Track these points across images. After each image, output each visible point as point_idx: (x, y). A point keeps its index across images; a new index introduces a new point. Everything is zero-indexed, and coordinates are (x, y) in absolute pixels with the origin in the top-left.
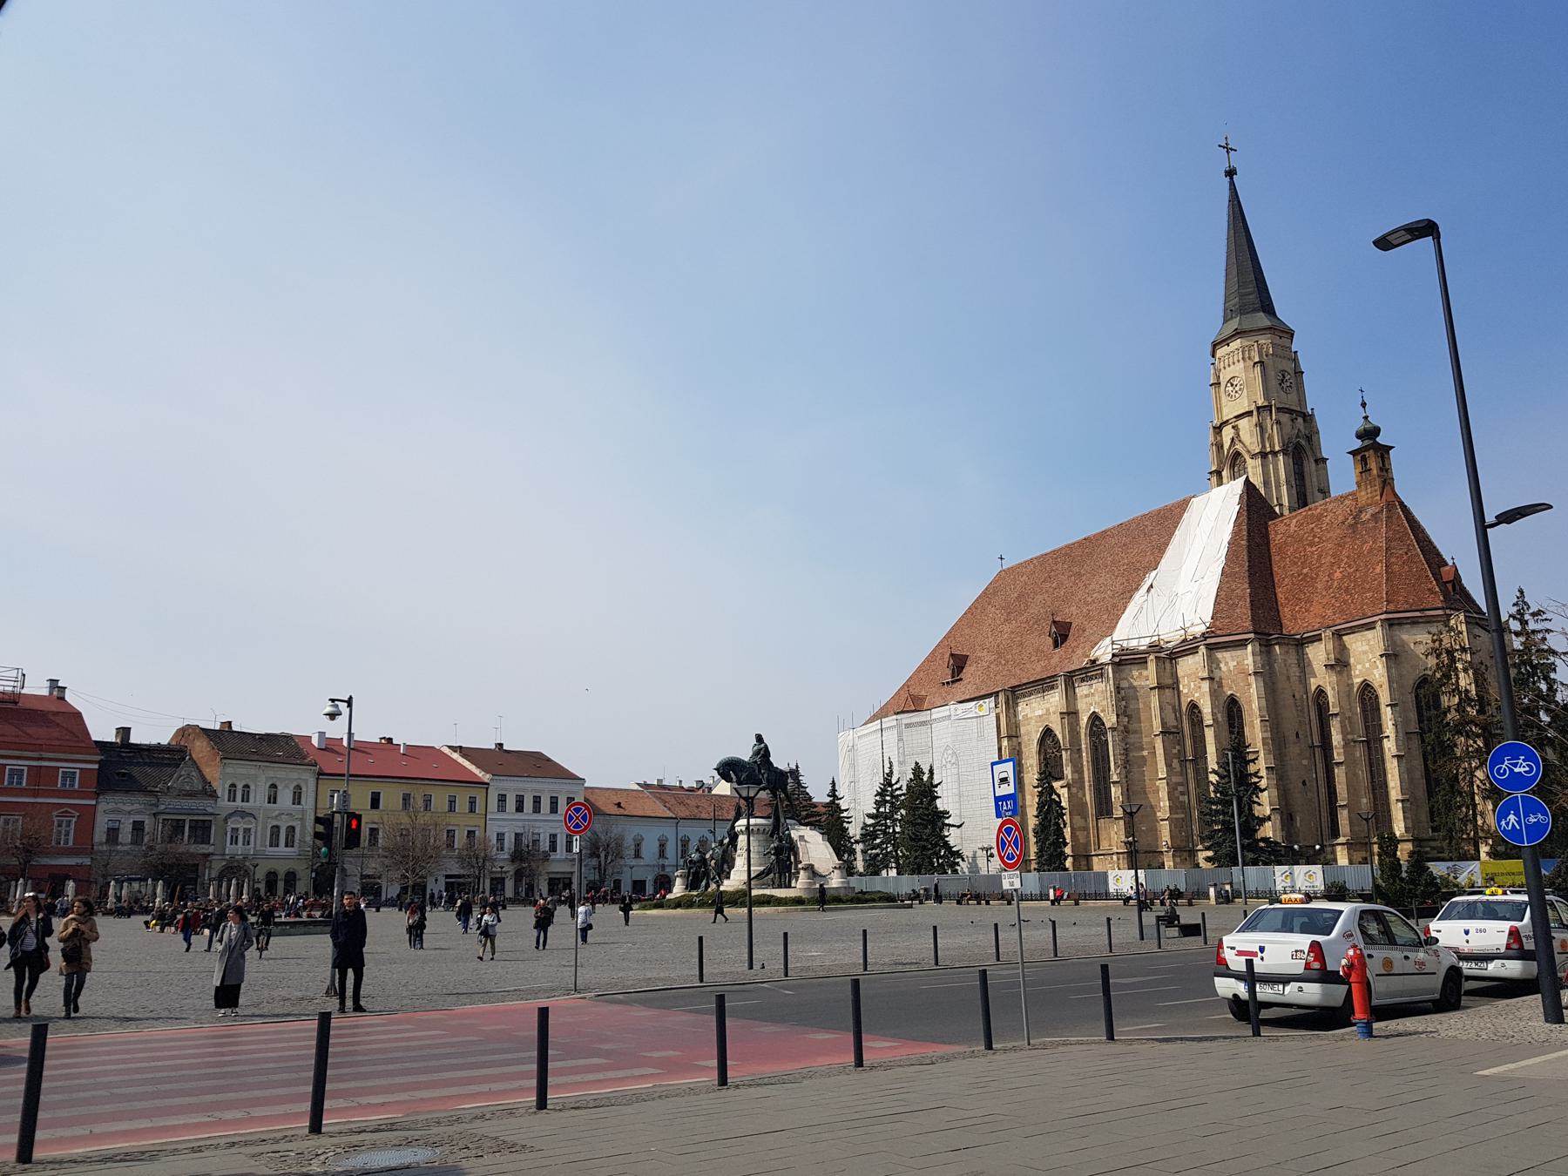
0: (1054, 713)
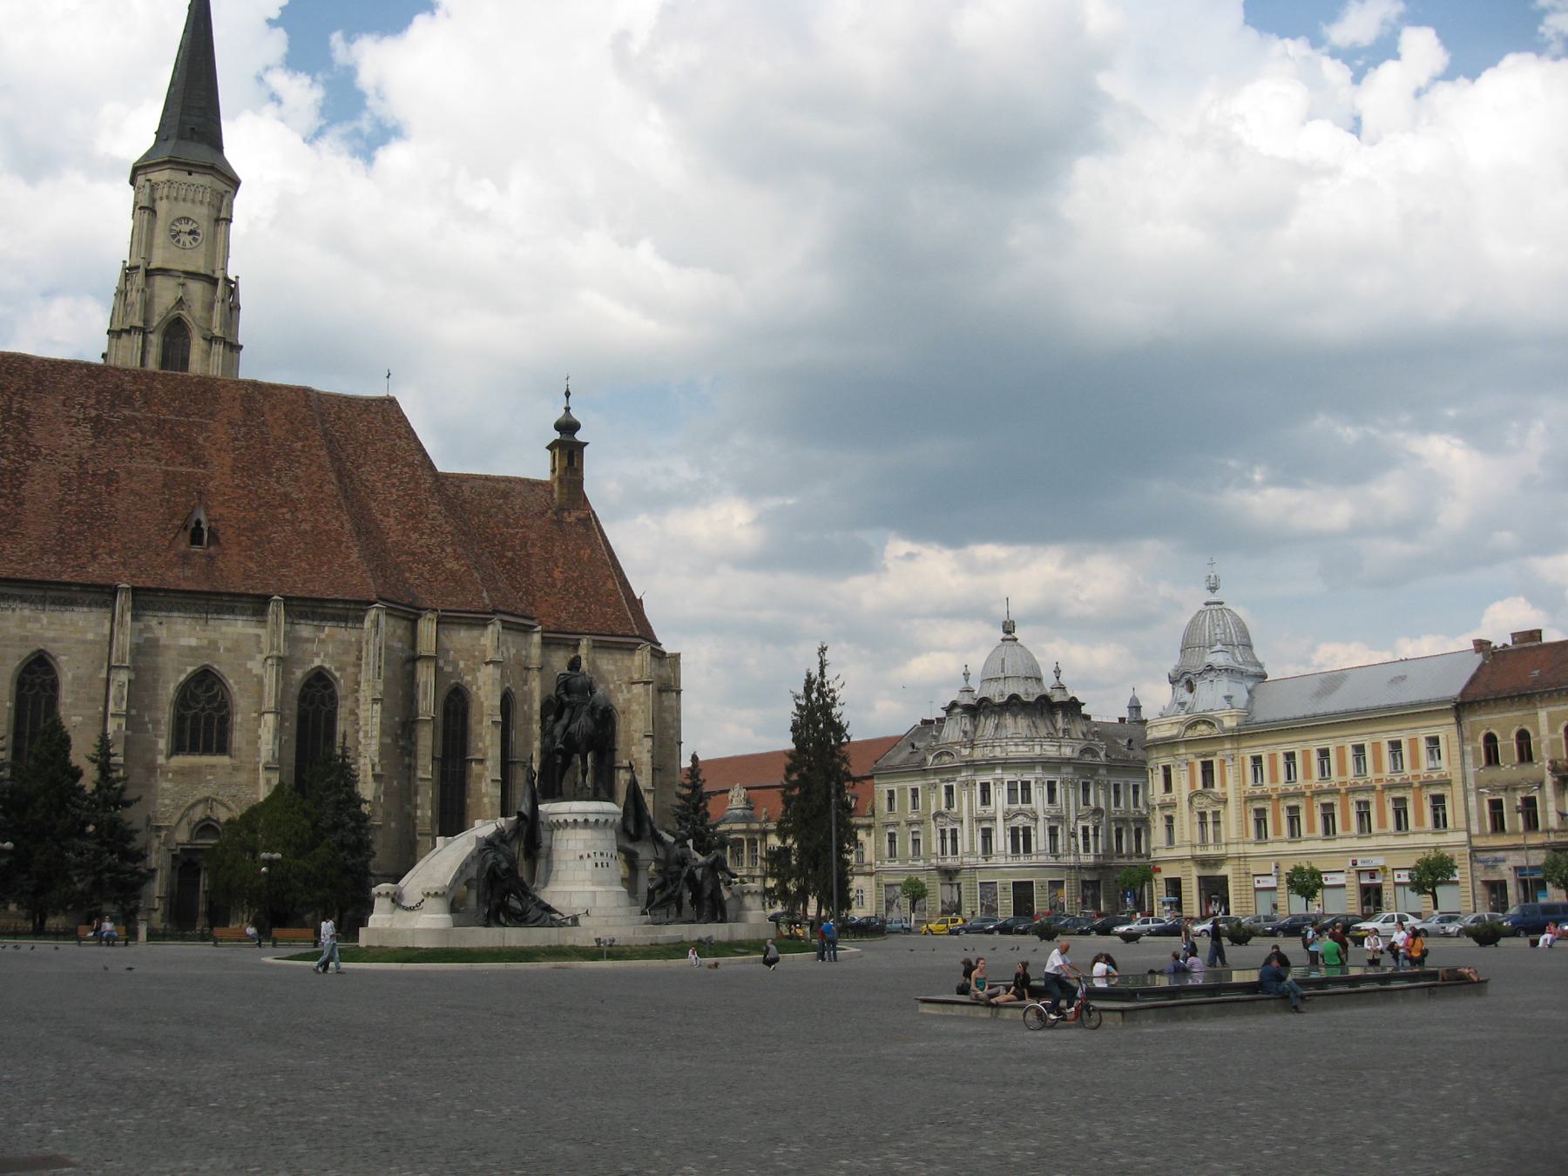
0: (228, 650)
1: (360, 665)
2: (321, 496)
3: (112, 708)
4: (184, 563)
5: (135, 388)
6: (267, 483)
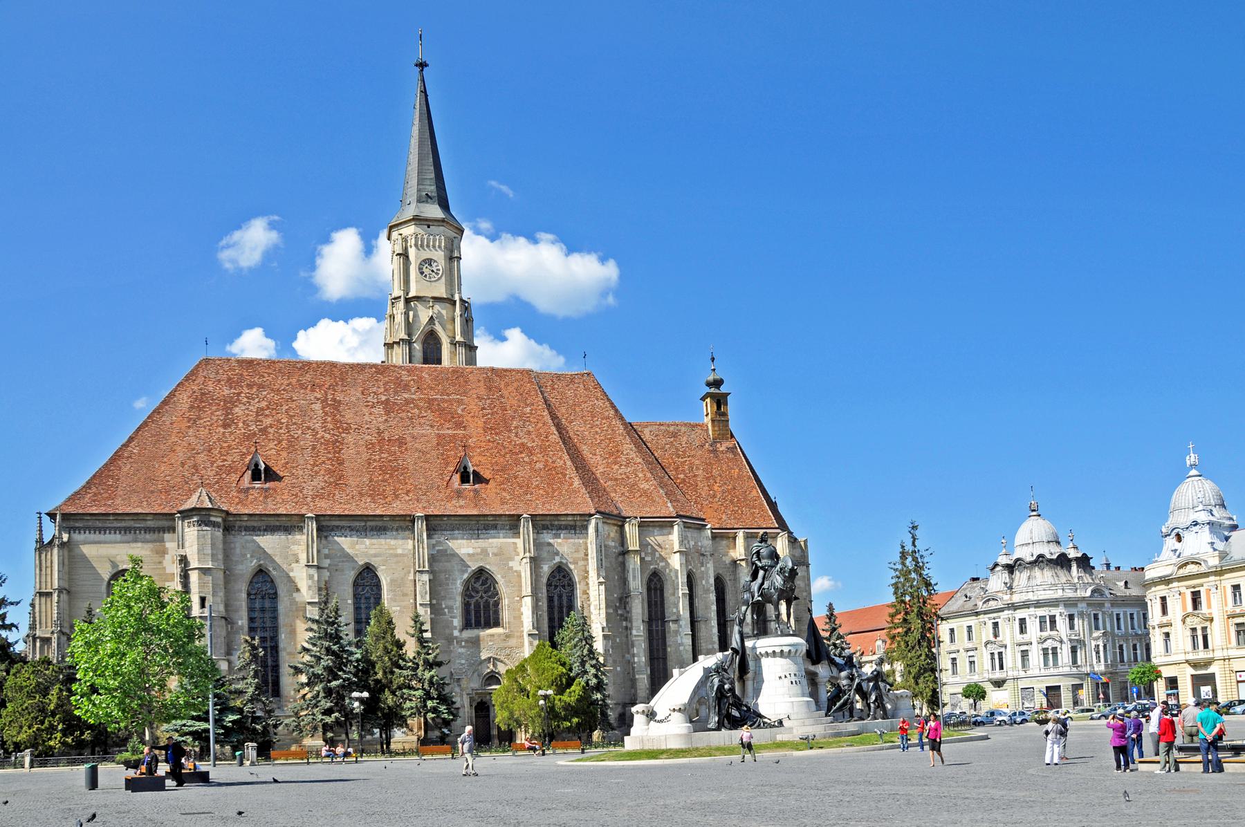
1: (587, 560)
2: (547, 444)
3: (419, 601)
4: (458, 497)
5: (410, 378)
6: (509, 437)
